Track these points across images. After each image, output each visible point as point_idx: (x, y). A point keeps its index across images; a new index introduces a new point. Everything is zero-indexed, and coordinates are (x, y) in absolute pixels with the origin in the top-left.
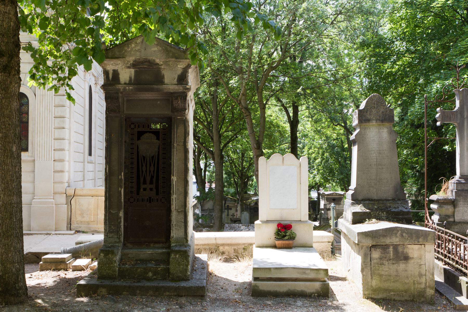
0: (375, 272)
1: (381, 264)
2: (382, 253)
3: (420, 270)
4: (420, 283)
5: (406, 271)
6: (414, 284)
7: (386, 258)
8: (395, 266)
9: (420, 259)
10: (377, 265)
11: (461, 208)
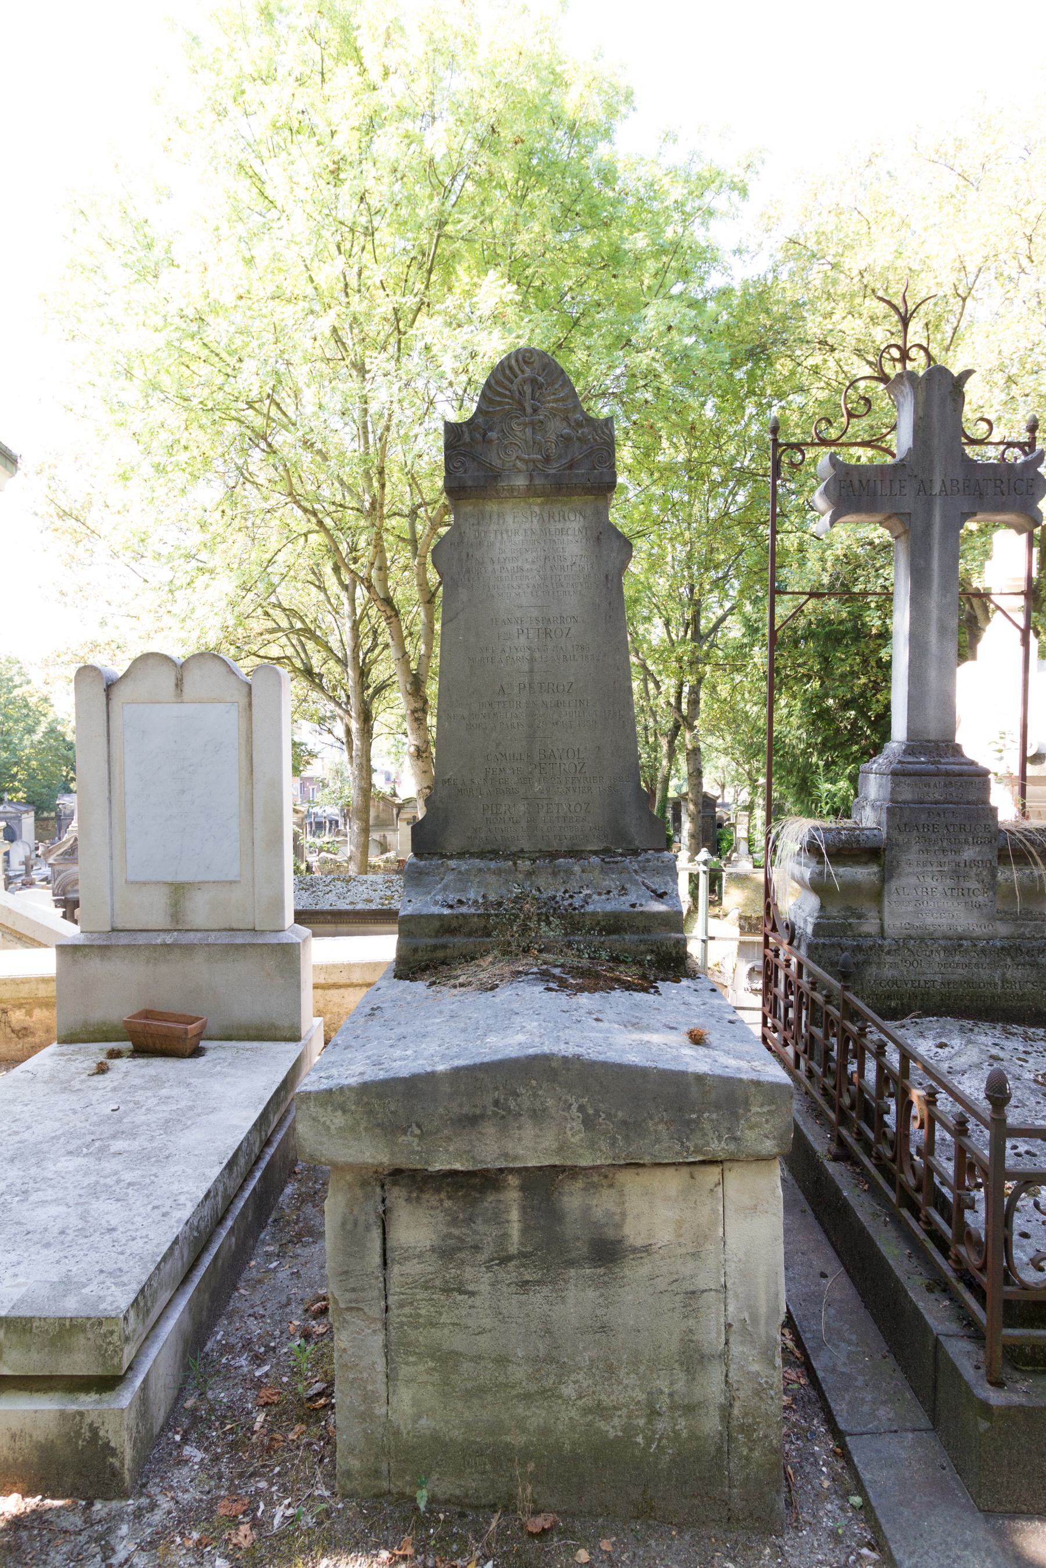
0: (412, 1334)
1: (446, 1290)
2: (454, 1222)
3: (691, 1322)
4: (690, 1409)
5: (603, 1328)
6: (653, 1413)
7: (476, 1248)
8: (538, 1299)
9: (695, 1255)
10: (421, 1295)
11: (913, 881)
